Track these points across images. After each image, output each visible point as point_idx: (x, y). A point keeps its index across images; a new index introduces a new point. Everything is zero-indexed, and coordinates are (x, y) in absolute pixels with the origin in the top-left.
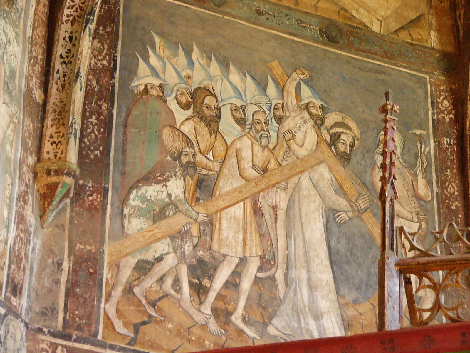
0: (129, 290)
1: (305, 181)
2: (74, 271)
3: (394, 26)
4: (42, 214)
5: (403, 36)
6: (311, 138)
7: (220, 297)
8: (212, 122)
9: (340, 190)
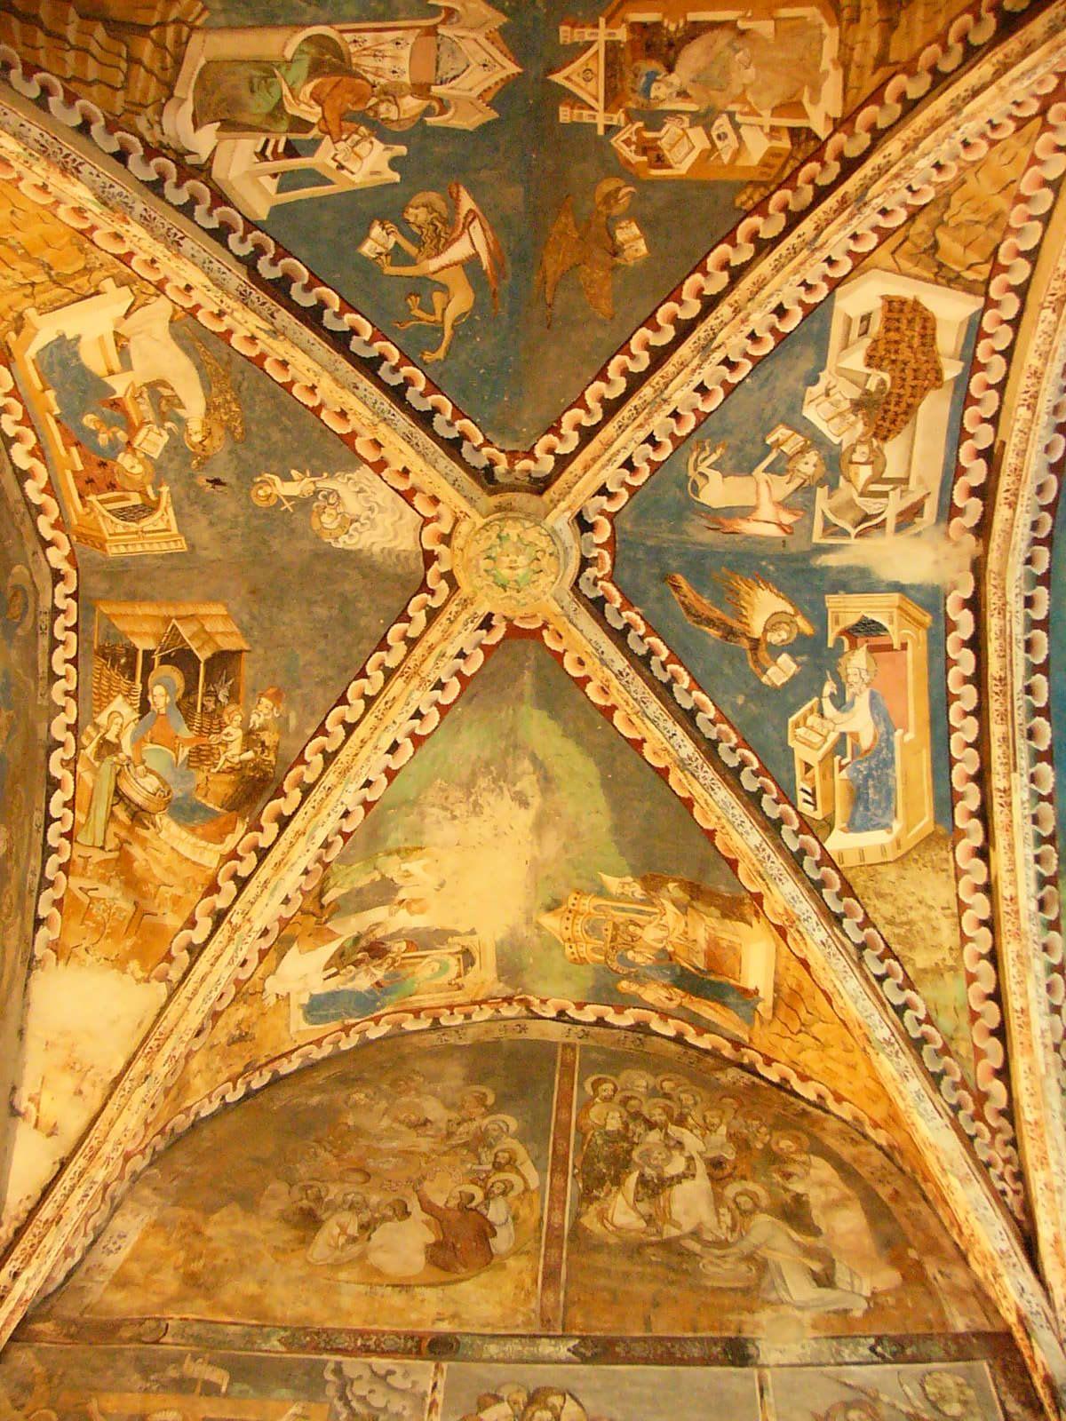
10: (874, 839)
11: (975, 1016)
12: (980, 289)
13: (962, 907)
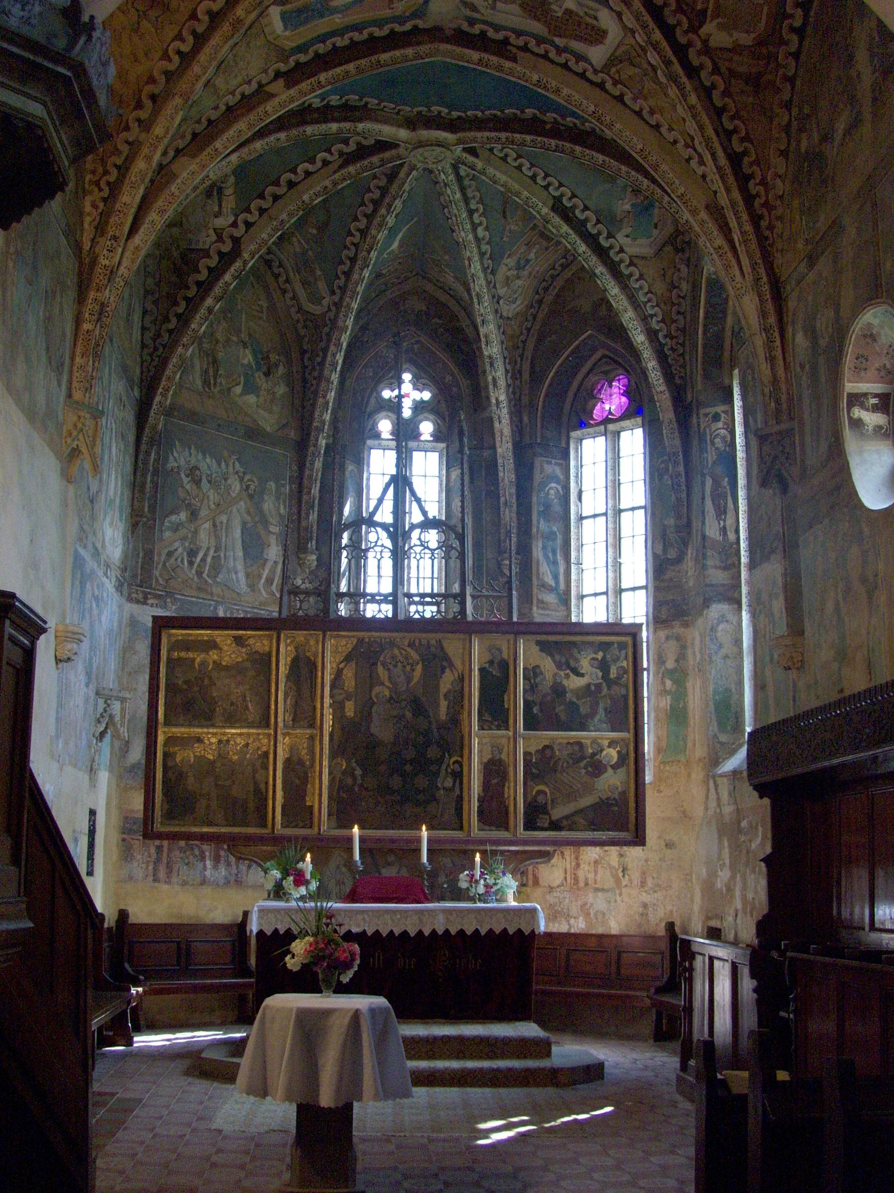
0: (165, 563)
1: (234, 510)
2: (144, 558)
3: (276, 427)
4: (133, 533)
6: (238, 487)
7: (199, 566)
8: (197, 482)
9: (249, 513)
10: (278, 25)
11: (199, 122)
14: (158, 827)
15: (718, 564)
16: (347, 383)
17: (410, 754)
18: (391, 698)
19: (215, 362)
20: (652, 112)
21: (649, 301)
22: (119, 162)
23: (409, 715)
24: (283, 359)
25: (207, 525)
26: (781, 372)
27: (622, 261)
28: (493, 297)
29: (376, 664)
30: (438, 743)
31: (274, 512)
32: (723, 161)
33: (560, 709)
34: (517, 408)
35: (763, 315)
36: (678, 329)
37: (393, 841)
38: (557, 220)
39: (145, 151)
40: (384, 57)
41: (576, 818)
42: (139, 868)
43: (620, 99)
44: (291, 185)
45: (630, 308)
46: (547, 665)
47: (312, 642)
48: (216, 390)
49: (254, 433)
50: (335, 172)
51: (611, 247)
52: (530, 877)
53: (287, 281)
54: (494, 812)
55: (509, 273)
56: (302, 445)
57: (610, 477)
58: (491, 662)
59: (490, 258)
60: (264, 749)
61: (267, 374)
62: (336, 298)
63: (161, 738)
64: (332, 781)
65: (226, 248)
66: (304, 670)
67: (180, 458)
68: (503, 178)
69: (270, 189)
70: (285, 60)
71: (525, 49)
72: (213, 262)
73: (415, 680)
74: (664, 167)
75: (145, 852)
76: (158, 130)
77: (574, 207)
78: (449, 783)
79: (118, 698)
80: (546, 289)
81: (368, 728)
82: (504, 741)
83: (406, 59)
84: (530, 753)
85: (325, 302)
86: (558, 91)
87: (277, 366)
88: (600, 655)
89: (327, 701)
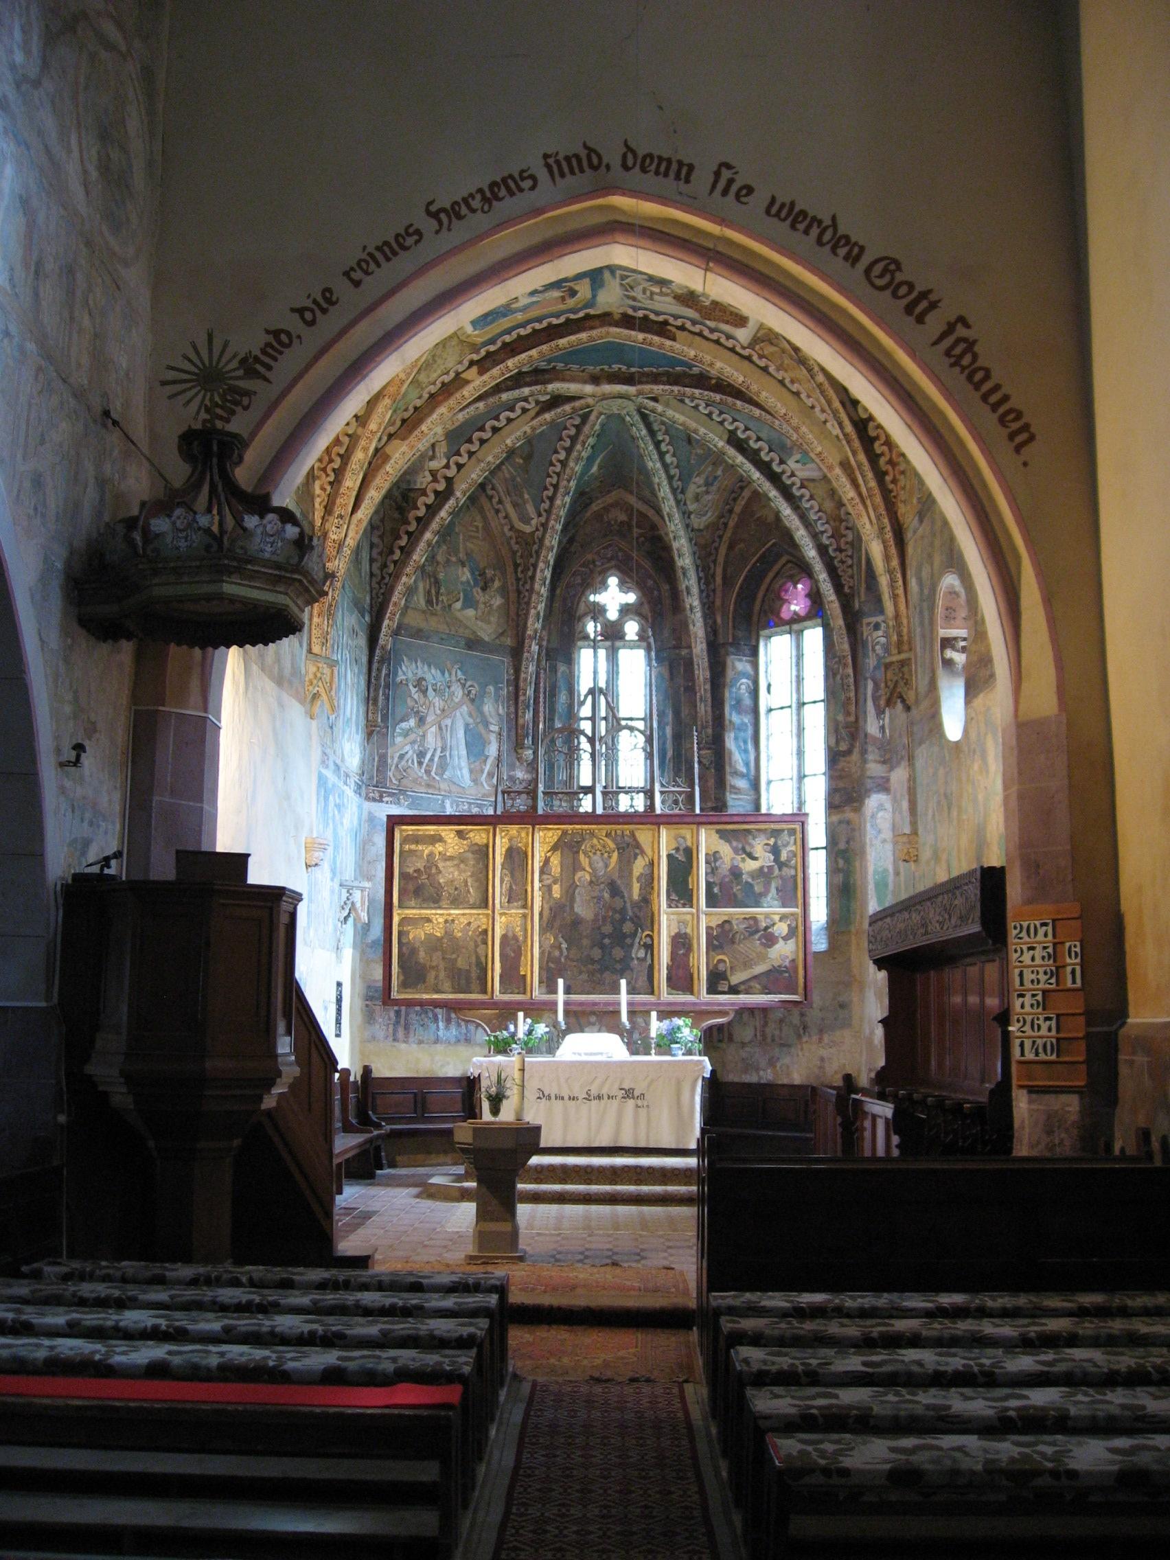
3: (494, 636)
5: (497, 642)
8: (424, 692)
9: (470, 715)
12: (751, 346)
13: (447, 373)
14: (395, 995)
15: (878, 758)
16: (558, 591)
17: (608, 929)
18: (591, 882)
19: (437, 583)
20: (792, 382)
21: (820, 519)
22: (342, 451)
23: (606, 896)
24: (497, 572)
25: (433, 729)
26: (902, 607)
27: (793, 484)
28: (684, 513)
29: (578, 852)
30: (631, 919)
31: (493, 713)
32: (849, 428)
33: (736, 889)
34: (709, 609)
35: (887, 558)
36: (847, 543)
37: (595, 1004)
38: (731, 451)
39: (363, 443)
40: (563, 342)
41: (752, 984)
42: (380, 1030)
43: (765, 369)
44: (495, 430)
45: (801, 527)
46: (725, 850)
47: (523, 835)
48: (438, 608)
49: (473, 643)
50: (533, 419)
51: (783, 472)
52: (726, 1035)
53: (500, 502)
54: (681, 979)
55: (699, 490)
56: (517, 653)
57: (794, 673)
58: (677, 849)
59: (680, 479)
60: (484, 927)
61: (484, 589)
62: (543, 519)
63: (396, 920)
64: (542, 953)
65: (441, 487)
66: (517, 858)
67: (408, 671)
68: (680, 418)
69: (476, 435)
70: (477, 352)
71: (682, 328)
72: (430, 499)
73: (612, 865)
74: (804, 429)
75: (385, 1017)
76: (373, 426)
77: (749, 438)
78: (641, 954)
79: (357, 888)
80: (735, 500)
81: (572, 908)
82: (689, 917)
83: (580, 342)
84: (711, 928)
85: (534, 522)
86: (711, 365)
87: (493, 580)
88: (772, 841)
89: (537, 884)
